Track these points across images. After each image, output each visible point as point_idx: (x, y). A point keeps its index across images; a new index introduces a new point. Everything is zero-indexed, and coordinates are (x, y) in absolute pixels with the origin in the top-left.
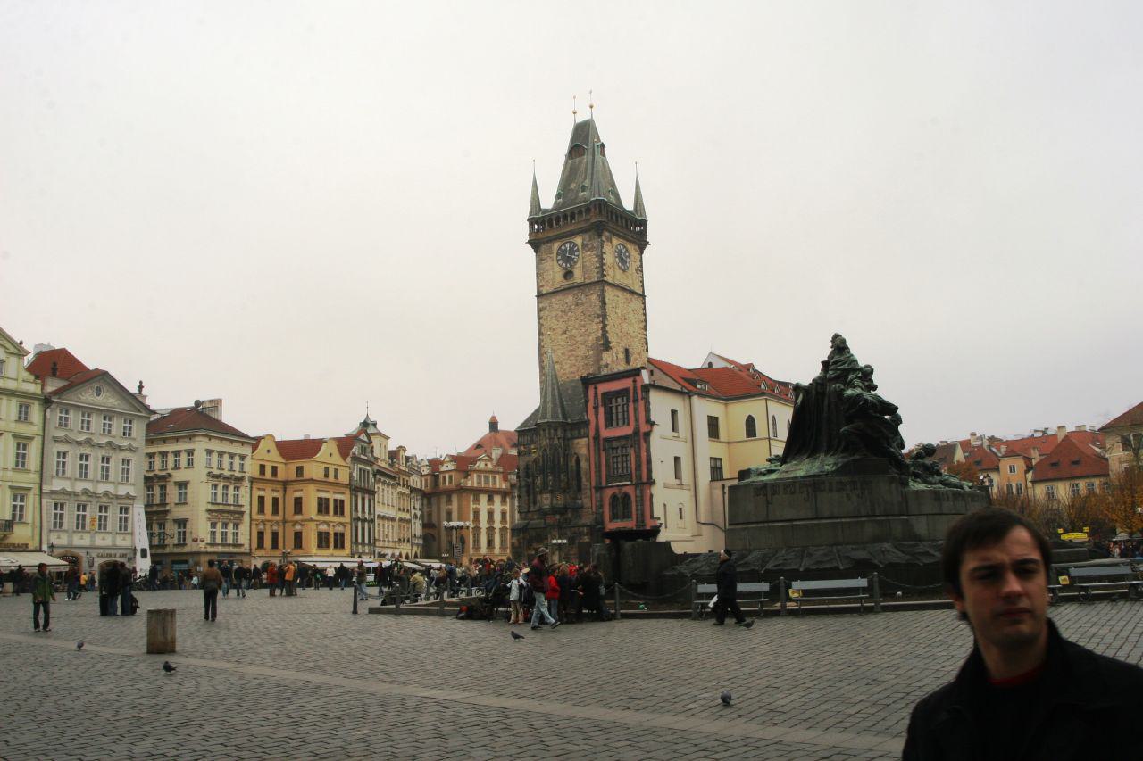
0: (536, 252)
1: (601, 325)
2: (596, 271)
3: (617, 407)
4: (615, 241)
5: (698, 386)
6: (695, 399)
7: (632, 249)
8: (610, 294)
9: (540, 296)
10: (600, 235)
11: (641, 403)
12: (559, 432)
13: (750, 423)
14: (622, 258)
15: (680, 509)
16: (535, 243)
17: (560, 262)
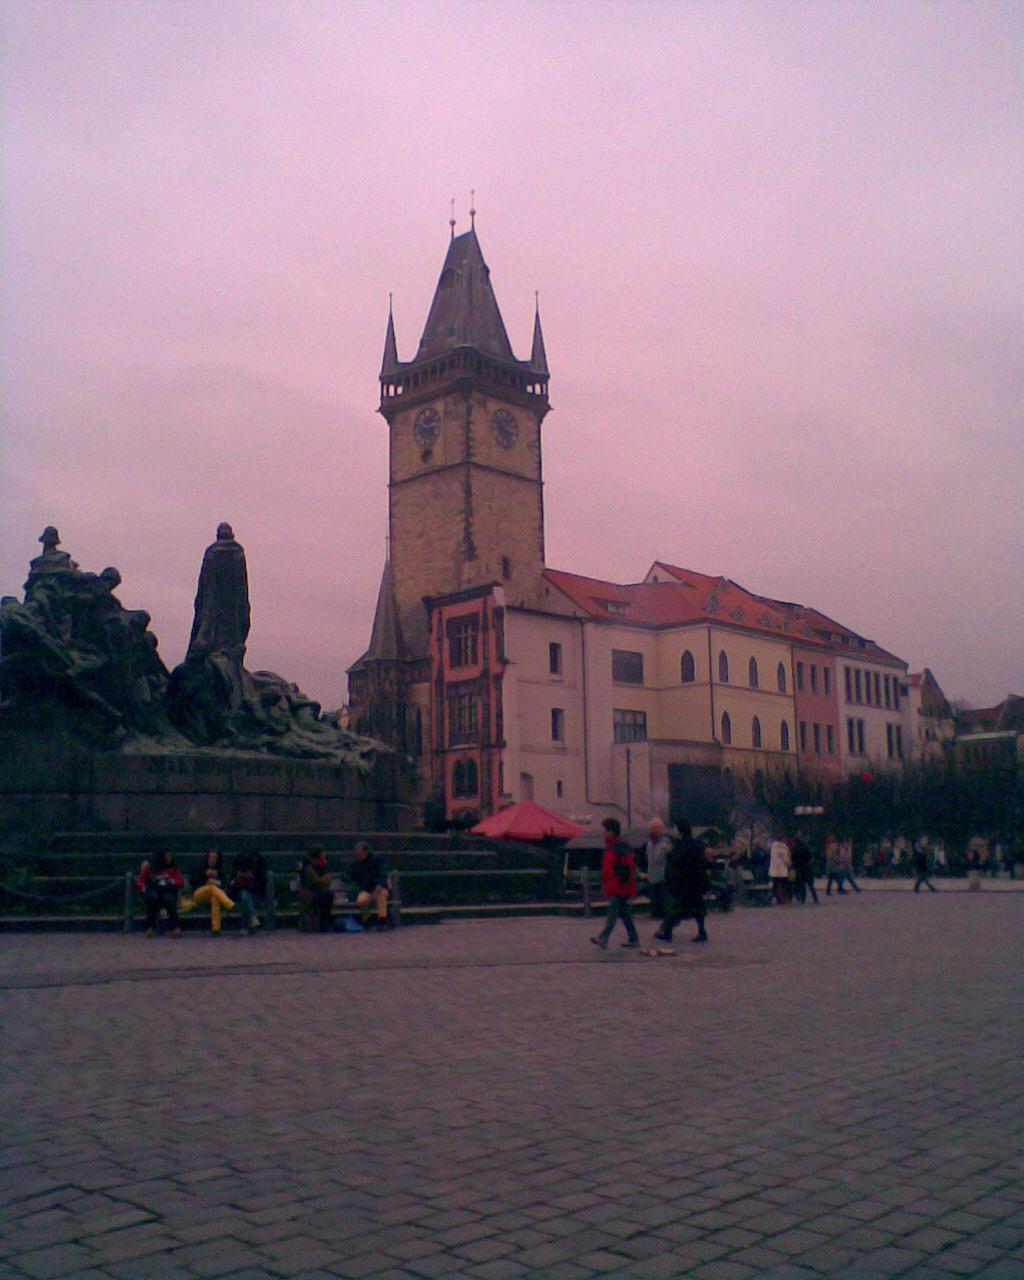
0: (389, 423)
1: (464, 524)
2: (461, 448)
3: (466, 639)
4: (493, 406)
5: (611, 609)
6: (589, 627)
7: (521, 415)
8: (479, 481)
9: (393, 485)
10: (466, 399)
11: (492, 633)
12: (392, 674)
13: (688, 662)
14: (505, 432)
15: (559, 784)
16: (389, 409)
17: (419, 437)
